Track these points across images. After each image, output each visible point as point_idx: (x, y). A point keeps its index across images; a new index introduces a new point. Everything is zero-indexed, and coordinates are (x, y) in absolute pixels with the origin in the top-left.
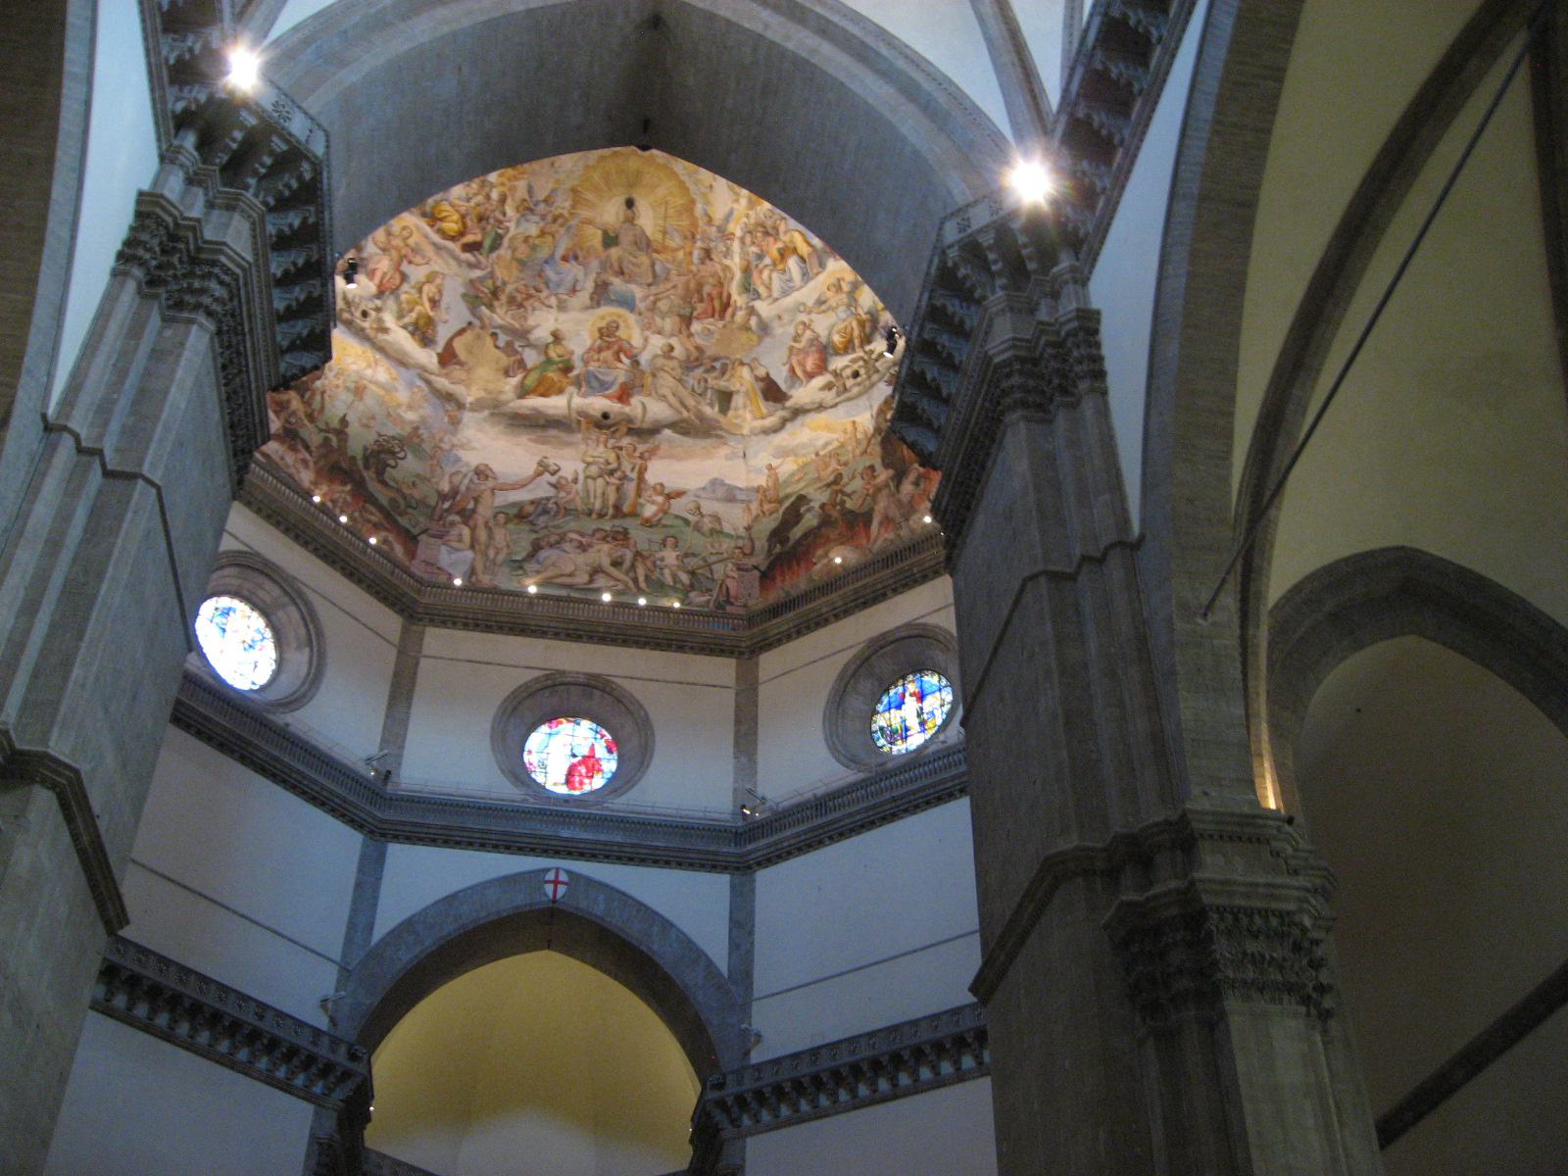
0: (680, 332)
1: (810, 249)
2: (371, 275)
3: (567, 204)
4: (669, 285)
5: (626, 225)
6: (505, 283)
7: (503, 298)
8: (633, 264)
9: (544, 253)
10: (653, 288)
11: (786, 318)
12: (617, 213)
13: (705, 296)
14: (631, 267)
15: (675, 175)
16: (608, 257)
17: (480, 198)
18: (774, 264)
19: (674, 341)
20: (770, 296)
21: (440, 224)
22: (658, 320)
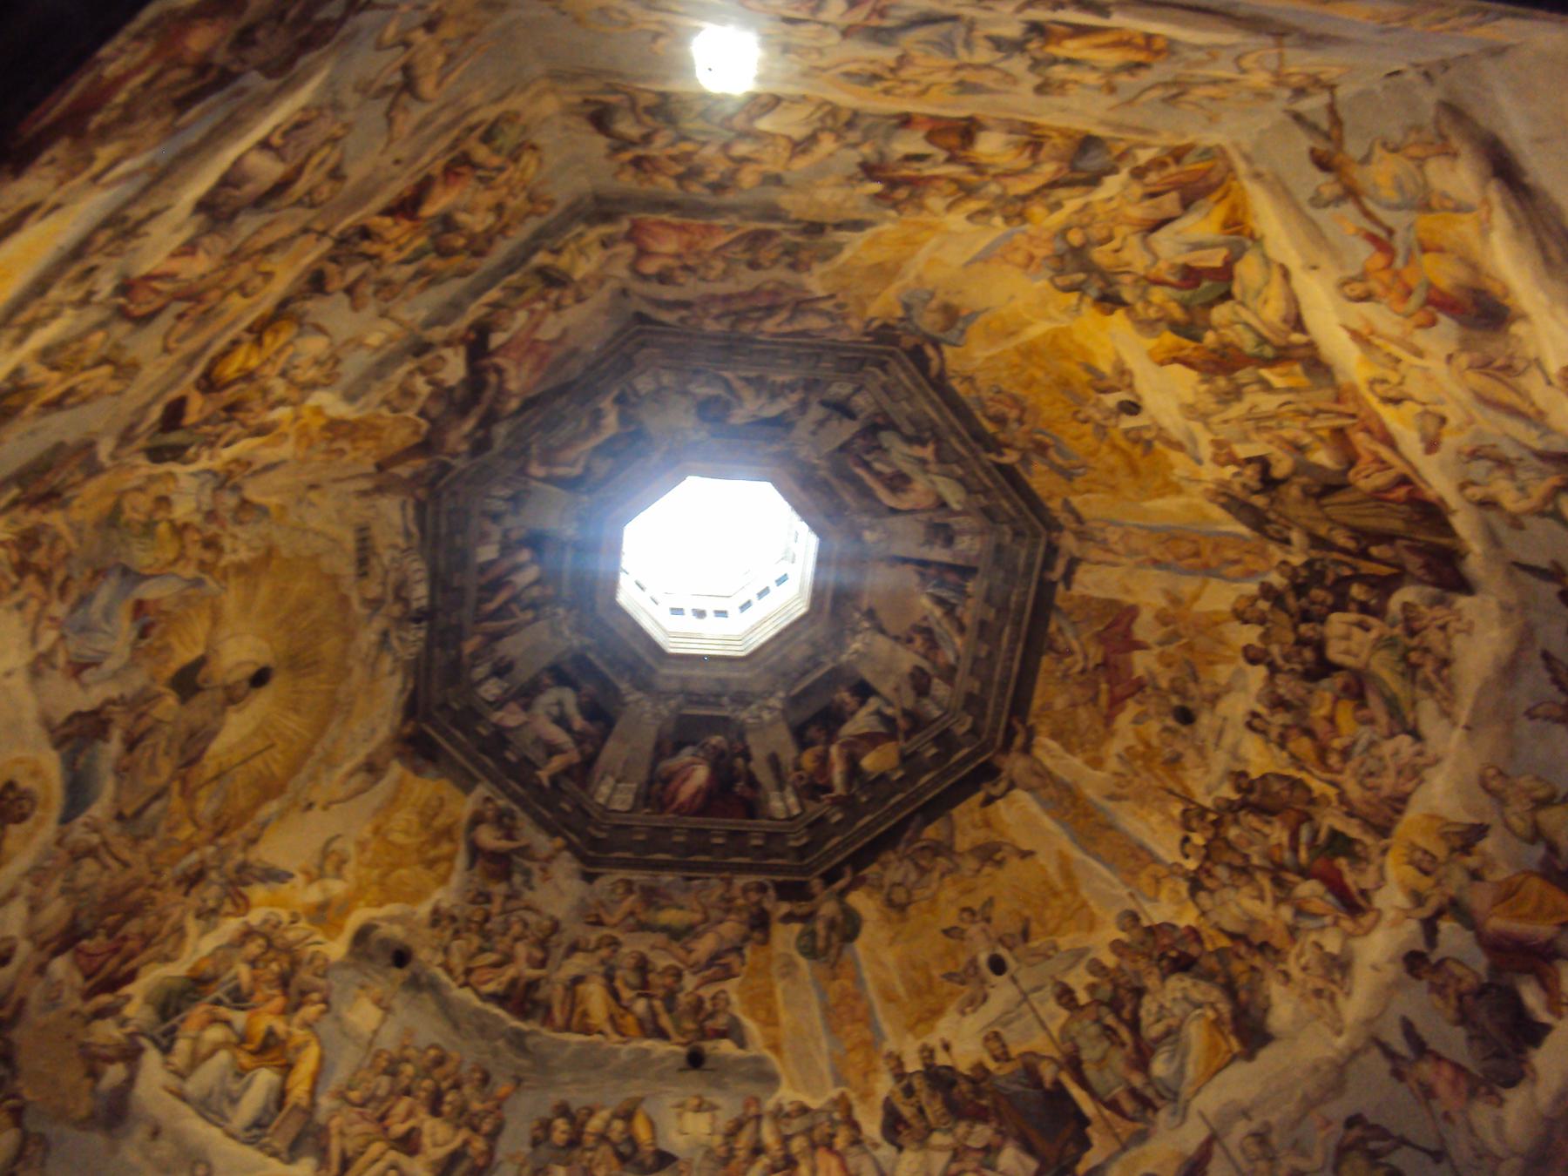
0: (44, 945)
1: (304, 1102)
2: (189, 249)
3: (244, 555)
4: (126, 855)
5: (220, 695)
6: (65, 505)
7: (33, 517)
8: (154, 755)
9: (142, 557)
10: (114, 828)
11: (164, 1149)
12: (239, 664)
13: (120, 934)
14: (149, 752)
15: (320, 729)
16: (159, 696)
17: (279, 387)
18: (243, 1039)
19: (24, 948)
20: (182, 1075)
21: (248, 337)
22: (57, 884)
